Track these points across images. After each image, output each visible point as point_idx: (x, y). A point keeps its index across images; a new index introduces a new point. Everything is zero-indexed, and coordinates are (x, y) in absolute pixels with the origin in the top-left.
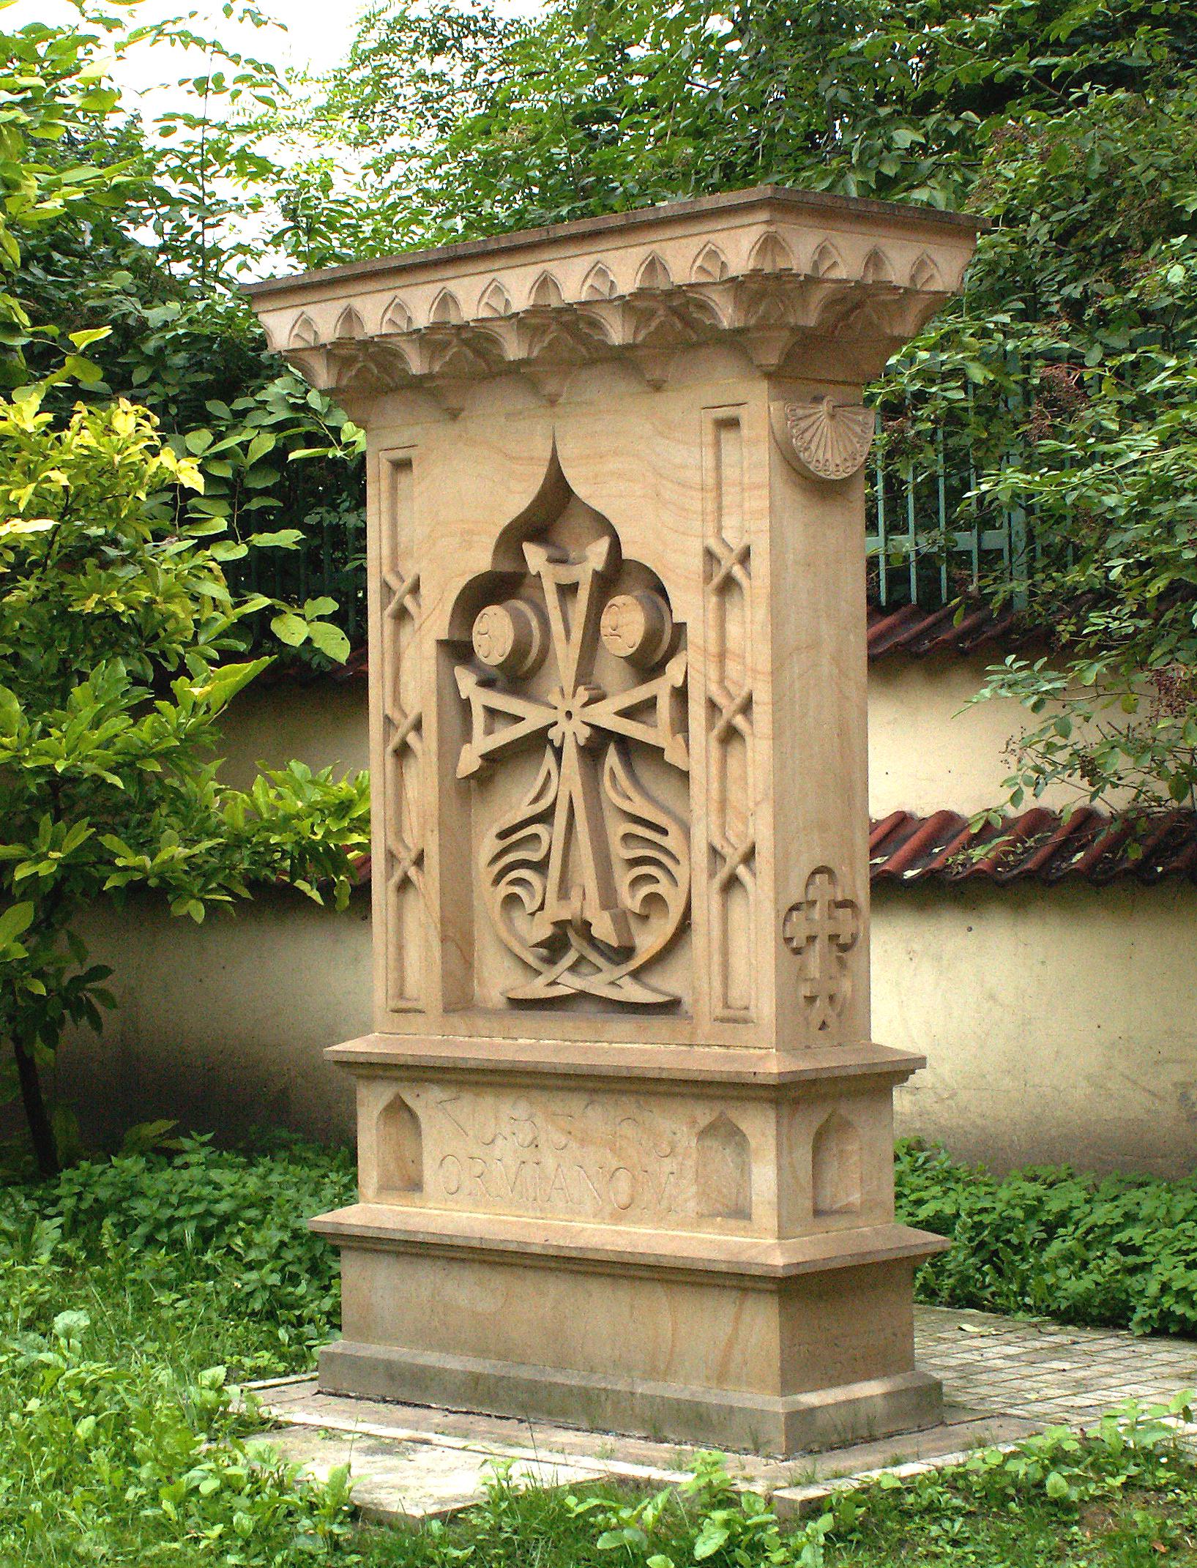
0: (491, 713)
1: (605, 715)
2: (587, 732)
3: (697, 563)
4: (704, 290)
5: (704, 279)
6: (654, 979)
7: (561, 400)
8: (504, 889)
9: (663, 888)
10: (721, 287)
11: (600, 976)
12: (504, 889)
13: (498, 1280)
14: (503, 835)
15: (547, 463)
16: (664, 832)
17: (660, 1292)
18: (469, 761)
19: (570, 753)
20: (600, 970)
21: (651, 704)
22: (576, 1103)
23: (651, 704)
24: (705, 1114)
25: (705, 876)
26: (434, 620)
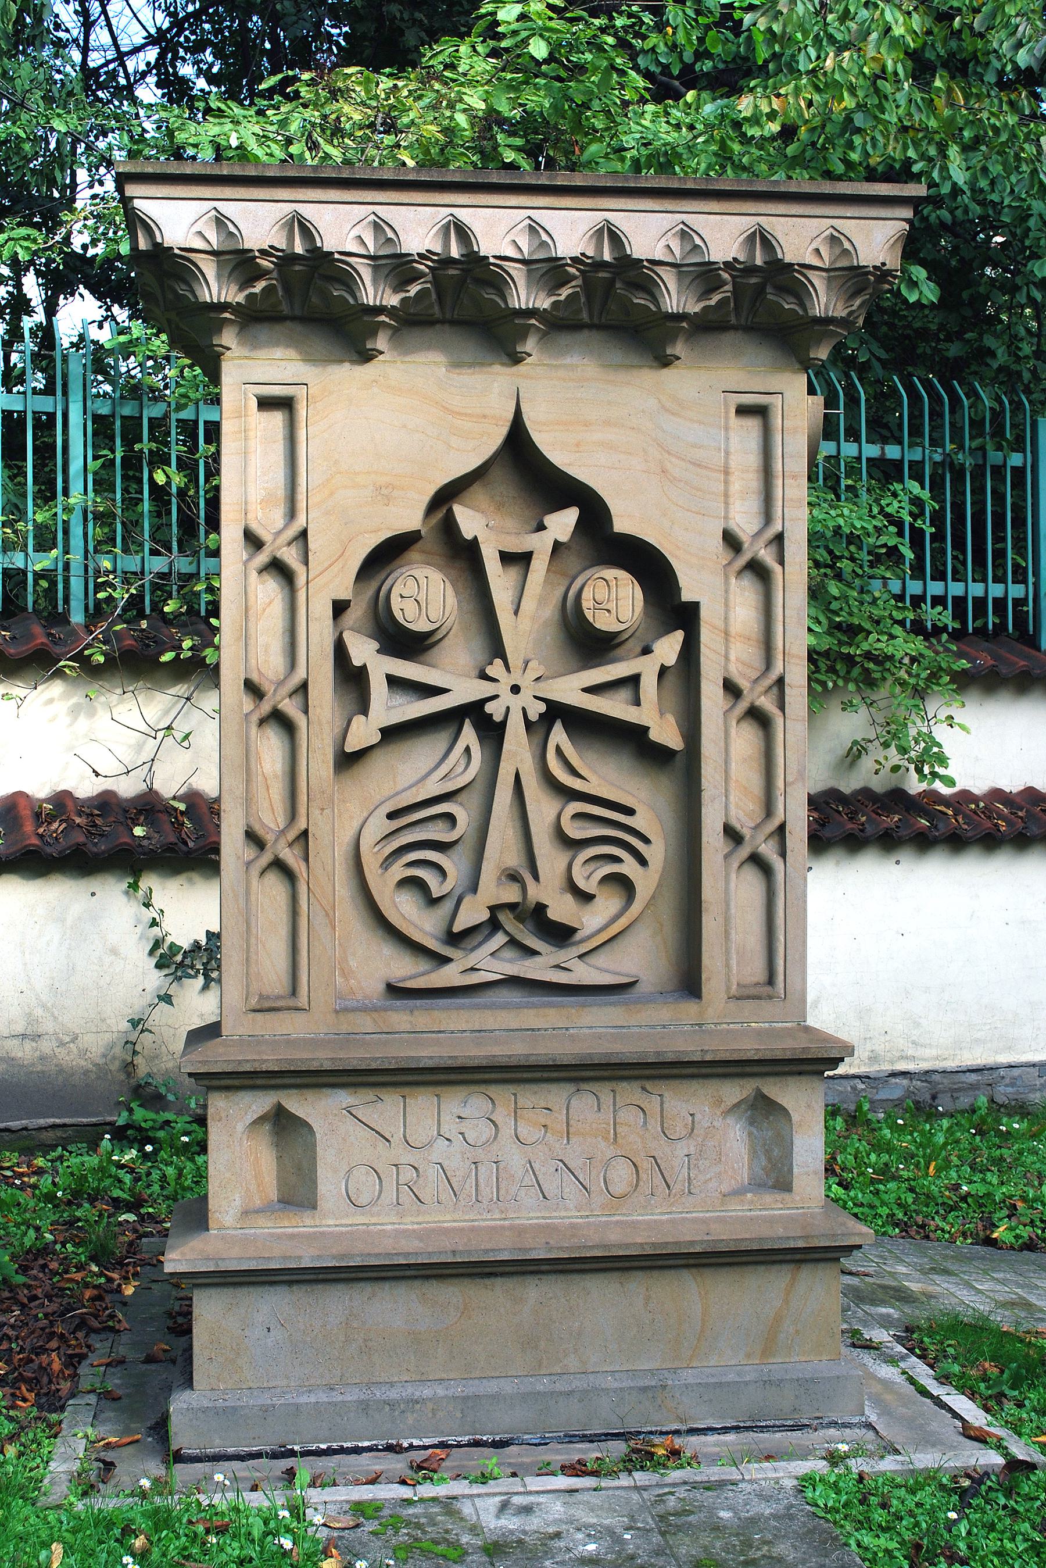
0: (394, 682)
1: (570, 689)
2: (542, 707)
3: (716, 542)
4: (811, 274)
5: (816, 262)
6: (600, 960)
7: (529, 360)
8: (398, 871)
9: (629, 867)
10: (824, 274)
11: (538, 959)
12: (398, 871)
13: (451, 1294)
14: (391, 816)
15: (509, 424)
16: (630, 812)
17: (686, 1275)
18: (363, 732)
19: (515, 730)
20: (534, 953)
21: (634, 680)
22: (556, 1095)
23: (634, 680)
24: (735, 1091)
25: (720, 858)
26: (332, 575)
